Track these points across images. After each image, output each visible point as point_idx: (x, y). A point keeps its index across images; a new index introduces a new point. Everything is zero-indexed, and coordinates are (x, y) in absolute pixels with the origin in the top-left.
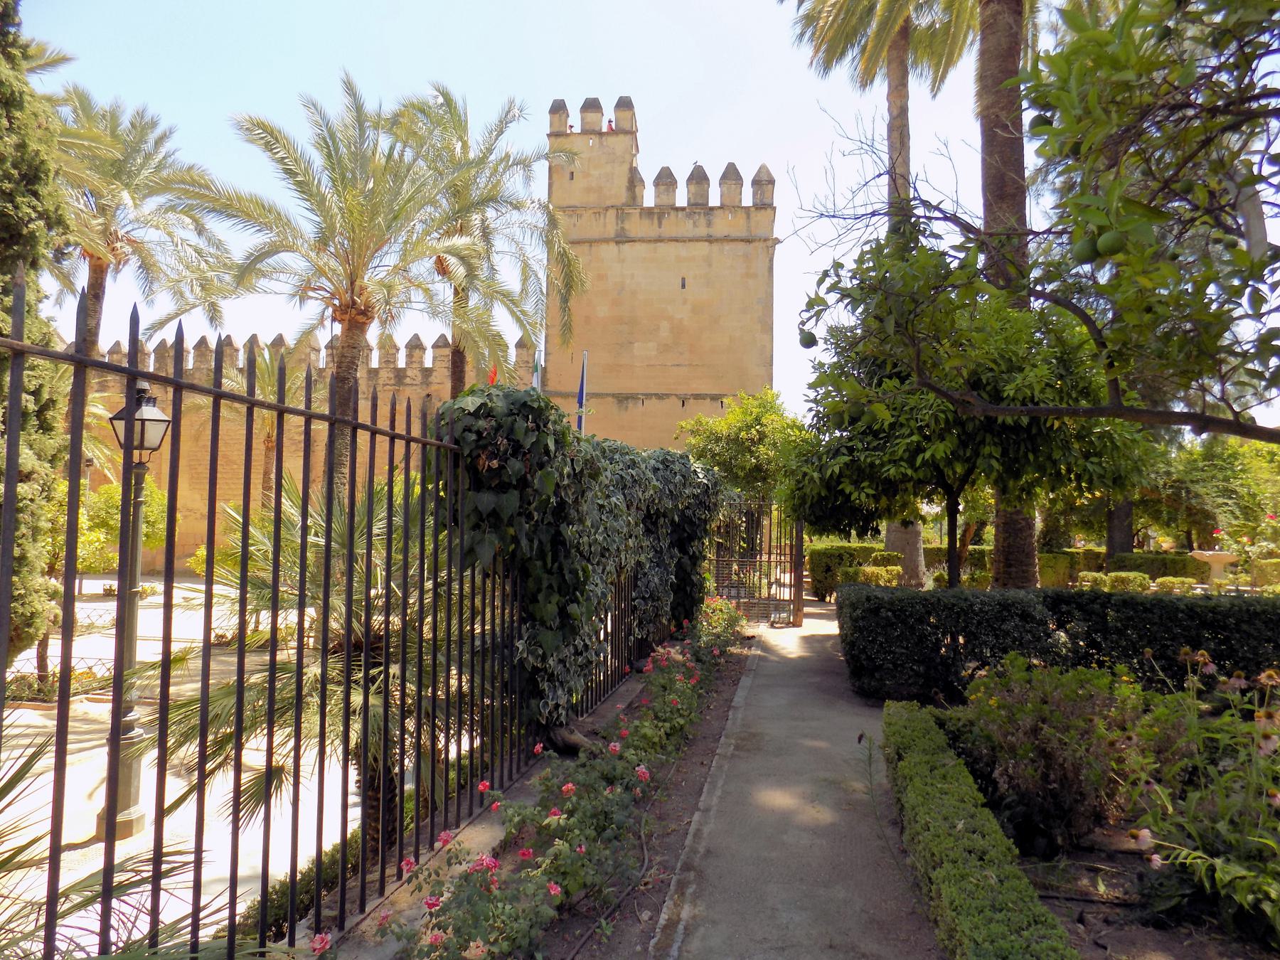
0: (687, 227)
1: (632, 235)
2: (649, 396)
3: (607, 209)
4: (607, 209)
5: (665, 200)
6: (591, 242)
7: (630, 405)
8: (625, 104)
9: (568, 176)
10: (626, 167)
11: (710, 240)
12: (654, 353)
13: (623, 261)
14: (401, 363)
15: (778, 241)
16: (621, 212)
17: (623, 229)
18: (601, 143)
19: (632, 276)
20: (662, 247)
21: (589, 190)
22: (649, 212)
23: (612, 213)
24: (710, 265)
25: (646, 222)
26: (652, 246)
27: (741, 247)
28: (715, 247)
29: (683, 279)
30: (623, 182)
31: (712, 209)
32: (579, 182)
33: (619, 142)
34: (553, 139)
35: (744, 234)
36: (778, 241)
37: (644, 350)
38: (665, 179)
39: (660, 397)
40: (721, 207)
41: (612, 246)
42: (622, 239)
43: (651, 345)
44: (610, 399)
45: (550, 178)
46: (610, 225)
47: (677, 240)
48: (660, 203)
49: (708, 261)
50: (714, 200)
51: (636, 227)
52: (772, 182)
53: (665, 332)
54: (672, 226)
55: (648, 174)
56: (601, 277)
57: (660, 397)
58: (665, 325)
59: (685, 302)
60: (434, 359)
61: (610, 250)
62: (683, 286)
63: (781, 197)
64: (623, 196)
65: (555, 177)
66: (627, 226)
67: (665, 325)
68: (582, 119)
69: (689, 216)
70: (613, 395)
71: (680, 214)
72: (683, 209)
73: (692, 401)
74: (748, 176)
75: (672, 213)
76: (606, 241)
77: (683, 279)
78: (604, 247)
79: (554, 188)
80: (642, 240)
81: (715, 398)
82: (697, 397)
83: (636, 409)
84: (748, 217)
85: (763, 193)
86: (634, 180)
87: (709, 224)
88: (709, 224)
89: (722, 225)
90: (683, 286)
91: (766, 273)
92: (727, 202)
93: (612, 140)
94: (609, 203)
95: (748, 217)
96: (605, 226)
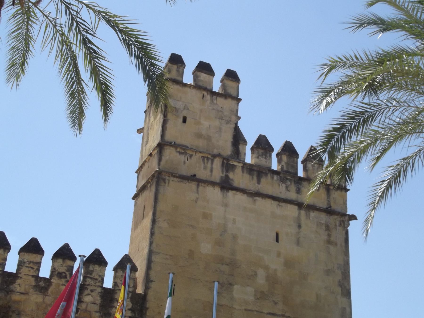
1: (236, 184)
3: (215, 156)
4: (215, 156)
8: (231, 76)
12: (252, 298)
17: (227, 177)
19: (234, 221)
20: (259, 200)
23: (217, 162)
24: (299, 226)
25: (247, 176)
29: (277, 235)
30: (229, 137)
38: (263, 145)
41: (217, 191)
42: (226, 185)
54: (268, 186)
56: (206, 216)
59: (279, 255)
61: (214, 193)
62: (277, 241)
64: (228, 150)
66: (231, 175)
71: (275, 177)
76: (213, 184)
77: (277, 235)
79: (169, 125)
80: (243, 191)
87: (298, 191)
88: (298, 191)
90: (277, 241)
91: (343, 244)
93: (220, 101)
94: (215, 152)
96: (211, 171)
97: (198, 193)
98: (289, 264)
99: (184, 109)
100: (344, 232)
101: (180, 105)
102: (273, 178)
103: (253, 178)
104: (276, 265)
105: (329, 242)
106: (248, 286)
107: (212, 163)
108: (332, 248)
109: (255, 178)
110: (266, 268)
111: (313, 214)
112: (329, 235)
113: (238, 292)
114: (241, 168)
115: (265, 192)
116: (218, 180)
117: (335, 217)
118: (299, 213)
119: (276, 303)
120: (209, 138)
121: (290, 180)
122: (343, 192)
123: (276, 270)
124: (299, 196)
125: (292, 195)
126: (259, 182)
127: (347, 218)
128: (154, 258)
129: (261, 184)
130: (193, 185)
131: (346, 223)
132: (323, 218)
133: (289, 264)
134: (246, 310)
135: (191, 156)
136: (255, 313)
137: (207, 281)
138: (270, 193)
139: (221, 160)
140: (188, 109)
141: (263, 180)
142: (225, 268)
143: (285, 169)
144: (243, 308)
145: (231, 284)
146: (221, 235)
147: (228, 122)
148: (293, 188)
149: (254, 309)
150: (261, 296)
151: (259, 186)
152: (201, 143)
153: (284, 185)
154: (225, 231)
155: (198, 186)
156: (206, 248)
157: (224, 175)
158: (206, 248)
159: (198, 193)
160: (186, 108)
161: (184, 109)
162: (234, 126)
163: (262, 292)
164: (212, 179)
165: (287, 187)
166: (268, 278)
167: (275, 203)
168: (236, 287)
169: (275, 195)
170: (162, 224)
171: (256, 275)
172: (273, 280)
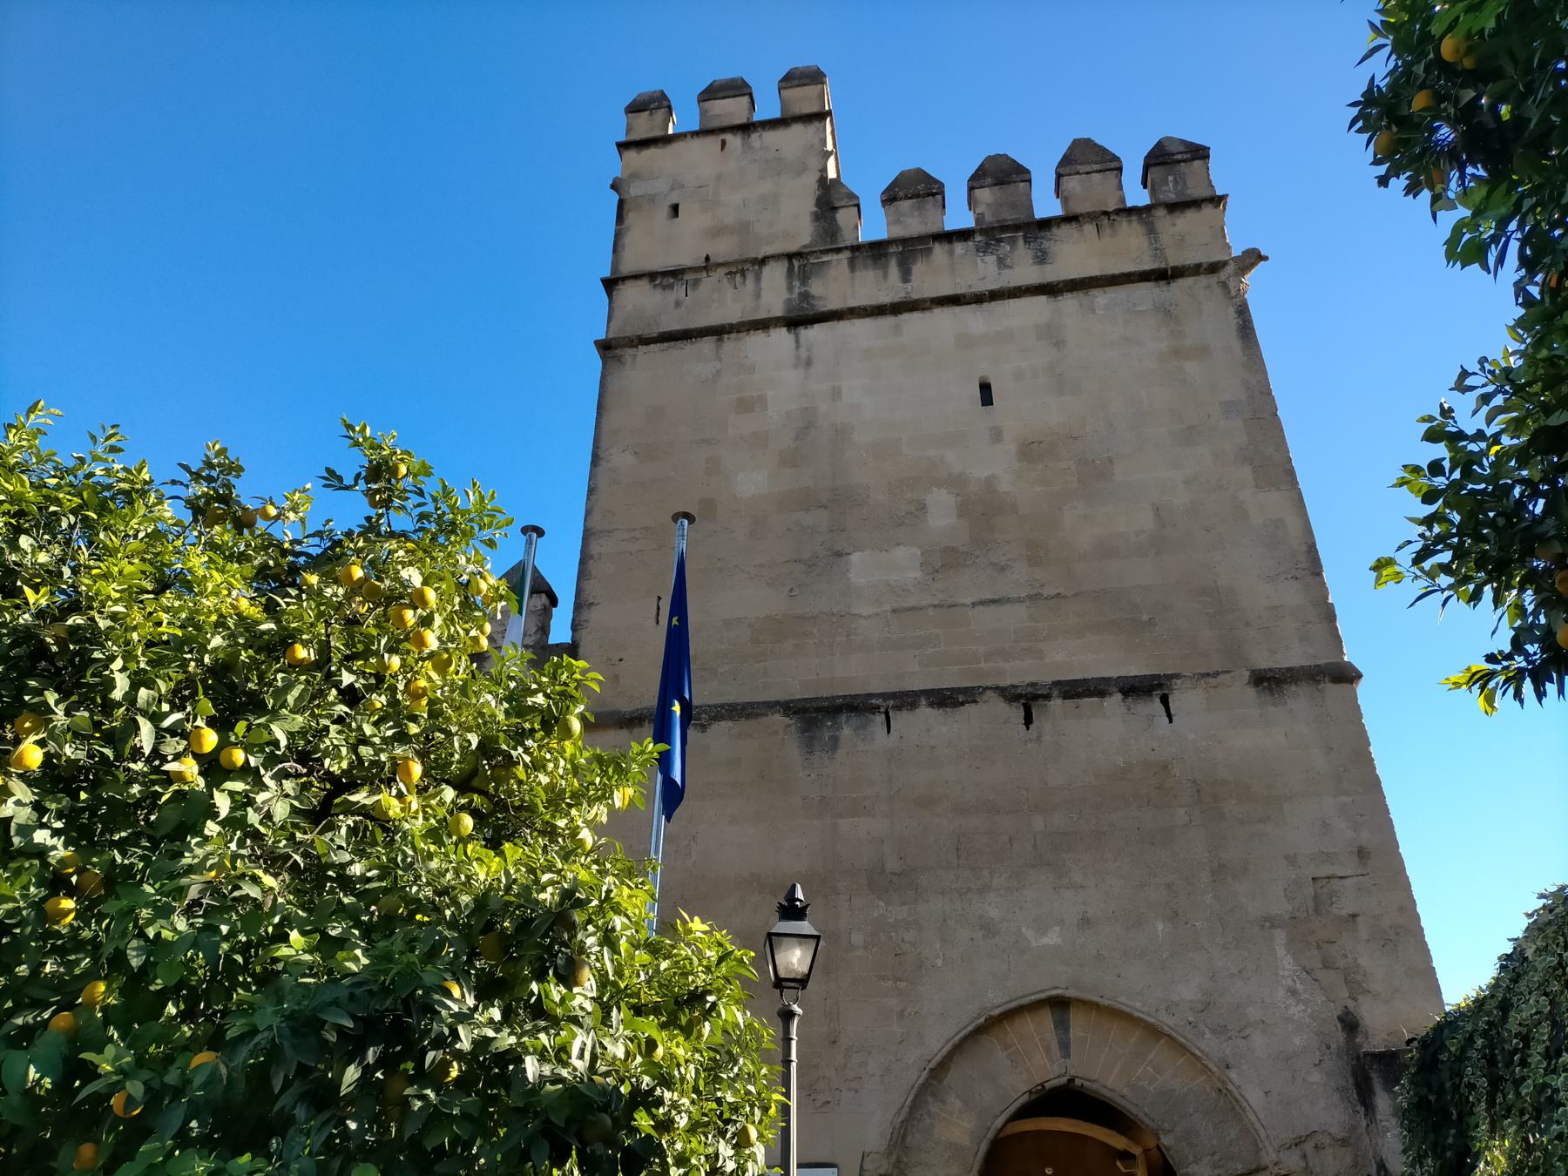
0: (982, 272)
2: (907, 700)
3: (763, 261)
4: (763, 261)
5: (914, 226)
6: (719, 332)
7: (846, 732)
9: (665, 211)
10: (811, 180)
12: (918, 574)
13: (809, 363)
16: (799, 262)
17: (805, 296)
18: (747, 146)
19: (836, 394)
21: (717, 232)
22: (876, 251)
23: (775, 275)
24: (1059, 344)
26: (887, 322)
27: (1145, 293)
28: (1069, 302)
29: (985, 388)
31: (1046, 224)
32: (694, 220)
33: (792, 139)
34: (631, 155)
35: (1148, 265)
37: (880, 571)
39: (945, 699)
40: (1070, 219)
41: (781, 336)
43: (901, 553)
44: (778, 719)
45: (620, 218)
46: (774, 291)
47: (955, 300)
48: (899, 232)
49: (1052, 336)
51: (838, 285)
53: (942, 514)
54: (937, 273)
55: (869, 185)
56: (745, 406)
57: (945, 699)
64: (802, 233)
65: (631, 218)
66: (816, 287)
68: (703, 113)
69: (984, 249)
70: (793, 708)
71: (959, 248)
72: (964, 235)
73: (1056, 704)
75: (939, 250)
76: (763, 325)
77: (985, 388)
78: (756, 339)
79: (628, 240)
81: (1134, 689)
82: (1075, 690)
83: (864, 748)
84: (1151, 231)
86: (831, 200)
87: (1042, 258)
88: (1042, 258)
89: (1075, 255)
91: (1236, 345)
93: (771, 137)
95: (1151, 231)
96: (757, 295)
97: (719, 359)
99: (672, 189)
100: (1231, 311)
101: (660, 186)
102: (951, 253)
103: (885, 276)
104: (995, 466)
105: (1177, 353)
106: (898, 544)
107: (758, 279)
108: (1192, 368)
109: (894, 270)
110: (956, 482)
113: (862, 568)
114: (845, 262)
116: (778, 310)
120: (744, 228)
121: (1012, 242)
122: (1208, 210)
123: (990, 482)
124: (1047, 268)
126: (906, 276)
127: (1230, 268)
128: (595, 548)
129: (913, 278)
130: (707, 344)
131: (1231, 284)
133: (1030, 451)
134: (894, 611)
135: (697, 282)
136: (931, 612)
137: (761, 566)
138: (947, 290)
139: (786, 263)
140: (683, 186)
141: (918, 268)
143: (989, 218)
144: (888, 608)
145: (839, 554)
146: (797, 438)
147: (801, 169)
149: (923, 603)
150: (945, 561)
151: (909, 286)
152: (724, 249)
153: (991, 259)
155: (720, 340)
156: (753, 481)
157: (795, 295)
158: (753, 481)
159: (719, 359)
160: (676, 185)
161: (672, 189)
162: (817, 175)
163: (950, 551)
164: (762, 315)
166: (963, 510)
169: (960, 290)
170: (620, 459)
171: (923, 508)
172: (983, 510)
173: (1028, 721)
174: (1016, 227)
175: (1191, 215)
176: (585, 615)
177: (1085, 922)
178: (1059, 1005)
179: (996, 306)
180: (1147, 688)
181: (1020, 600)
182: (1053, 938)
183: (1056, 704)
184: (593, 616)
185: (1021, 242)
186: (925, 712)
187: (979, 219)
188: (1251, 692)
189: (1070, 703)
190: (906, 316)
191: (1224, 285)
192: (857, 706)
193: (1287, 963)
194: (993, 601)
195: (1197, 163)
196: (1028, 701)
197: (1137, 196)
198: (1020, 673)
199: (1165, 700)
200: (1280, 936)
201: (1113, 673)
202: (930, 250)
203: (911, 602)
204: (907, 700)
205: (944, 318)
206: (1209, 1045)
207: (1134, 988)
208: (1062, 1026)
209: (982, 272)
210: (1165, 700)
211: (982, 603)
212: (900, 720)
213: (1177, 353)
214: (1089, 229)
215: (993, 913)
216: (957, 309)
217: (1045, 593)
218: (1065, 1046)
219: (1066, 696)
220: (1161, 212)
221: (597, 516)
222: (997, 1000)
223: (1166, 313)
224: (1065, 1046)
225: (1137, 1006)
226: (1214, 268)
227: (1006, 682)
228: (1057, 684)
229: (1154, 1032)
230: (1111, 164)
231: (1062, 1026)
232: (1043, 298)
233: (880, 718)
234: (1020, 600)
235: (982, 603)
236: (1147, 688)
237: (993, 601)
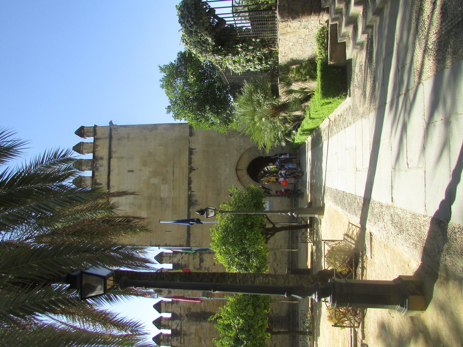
0: (103, 170)
2: (190, 189)
7: (194, 199)
11: (110, 158)
12: (167, 186)
14: (169, 332)
15: (111, 123)
20: (111, 184)
24: (122, 158)
28: (113, 155)
29: (129, 171)
35: (108, 141)
36: (111, 123)
37: (165, 191)
39: (190, 182)
40: (94, 152)
44: (191, 210)
50: (90, 156)
52: (82, 128)
53: (155, 181)
57: (190, 182)
58: (153, 181)
59: (140, 170)
60: (167, 312)
63: (89, 124)
67: (153, 181)
69: (97, 169)
70: (189, 208)
71: (96, 174)
73: (192, 165)
74: (79, 140)
77: (129, 171)
82: (190, 162)
85: (88, 132)
87: (102, 158)
88: (102, 158)
89: (103, 152)
92: (92, 150)
98: (145, 164)
102: (97, 175)
110: (149, 178)
111: (114, 149)
112: (124, 138)
113: (165, 194)
115: (107, 180)
117: (113, 134)
118: (115, 157)
119: (167, 171)
122: (97, 128)
123: (149, 172)
124: (104, 158)
125: (105, 162)
127: (111, 127)
128: (154, 244)
132: (114, 142)
133: (145, 164)
138: (106, 177)
142: (153, 202)
145: (161, 199)
148: (100, 162)
150: (165, 181)
153: (100, 168)
154: (133, 204)
163: (163, 180)
165: (101, 166)
167: (112, 174)
168: (162, 196)
169: (107, 174)
171: (154, 184)
172: (155, 174)
173: (195, 170)
174: (94, 162)
175: (97, 132)
176: (168, 245)
177: (226, 165)
178: (237, 170)
179: (112, 168)
180: (191, 152)
181: (173, 169)
182: (228, 170)
183: (192, 165)
184: (168, 243)
185: (97, 162)
186: (192, 185)
187: (90, 170)
188: (192, 137)
189: (192, 163)
190: (111, 185)
191: (115, 128)
192: (190, 197)
193: (232, 139)
194: (173, 173)
195: (85, 128)
196: (191, 170)
197: (90, 140)
198: (186, 171)
199: (193, 149)
200: (229, 139)
201: (188, 156)
202: (95, 179)
203: (172, 187)
204: (190, 189)
205: (112, 177)
206: (242, 151)
207: (235, 159)
208: (239, 170)
209: (103, 170)
210: (193, 149)
211: (173, 175)
212: (193, 190)
213: (128, 138)
214: (96, 150)
215: (224, 177)
216: (111, 175)
217: (172, 164)
218: (242, 170)
219: (191, 164)
220: (96, 137)
221: (147, 244)
222: (236, 178)
223: (120, 139)
224: (242, 170)
225: (237, 159)
226: (111, 129)
227: (188, 172)
228: (189, 165)
229: (240, 158)
230: (81, 144)
231: (239, 170)
232: (112, 160)
233: (192, 193)
234: (173, 169)
235: (173, 175)
236: (191, 152)
237: (173, 173)
